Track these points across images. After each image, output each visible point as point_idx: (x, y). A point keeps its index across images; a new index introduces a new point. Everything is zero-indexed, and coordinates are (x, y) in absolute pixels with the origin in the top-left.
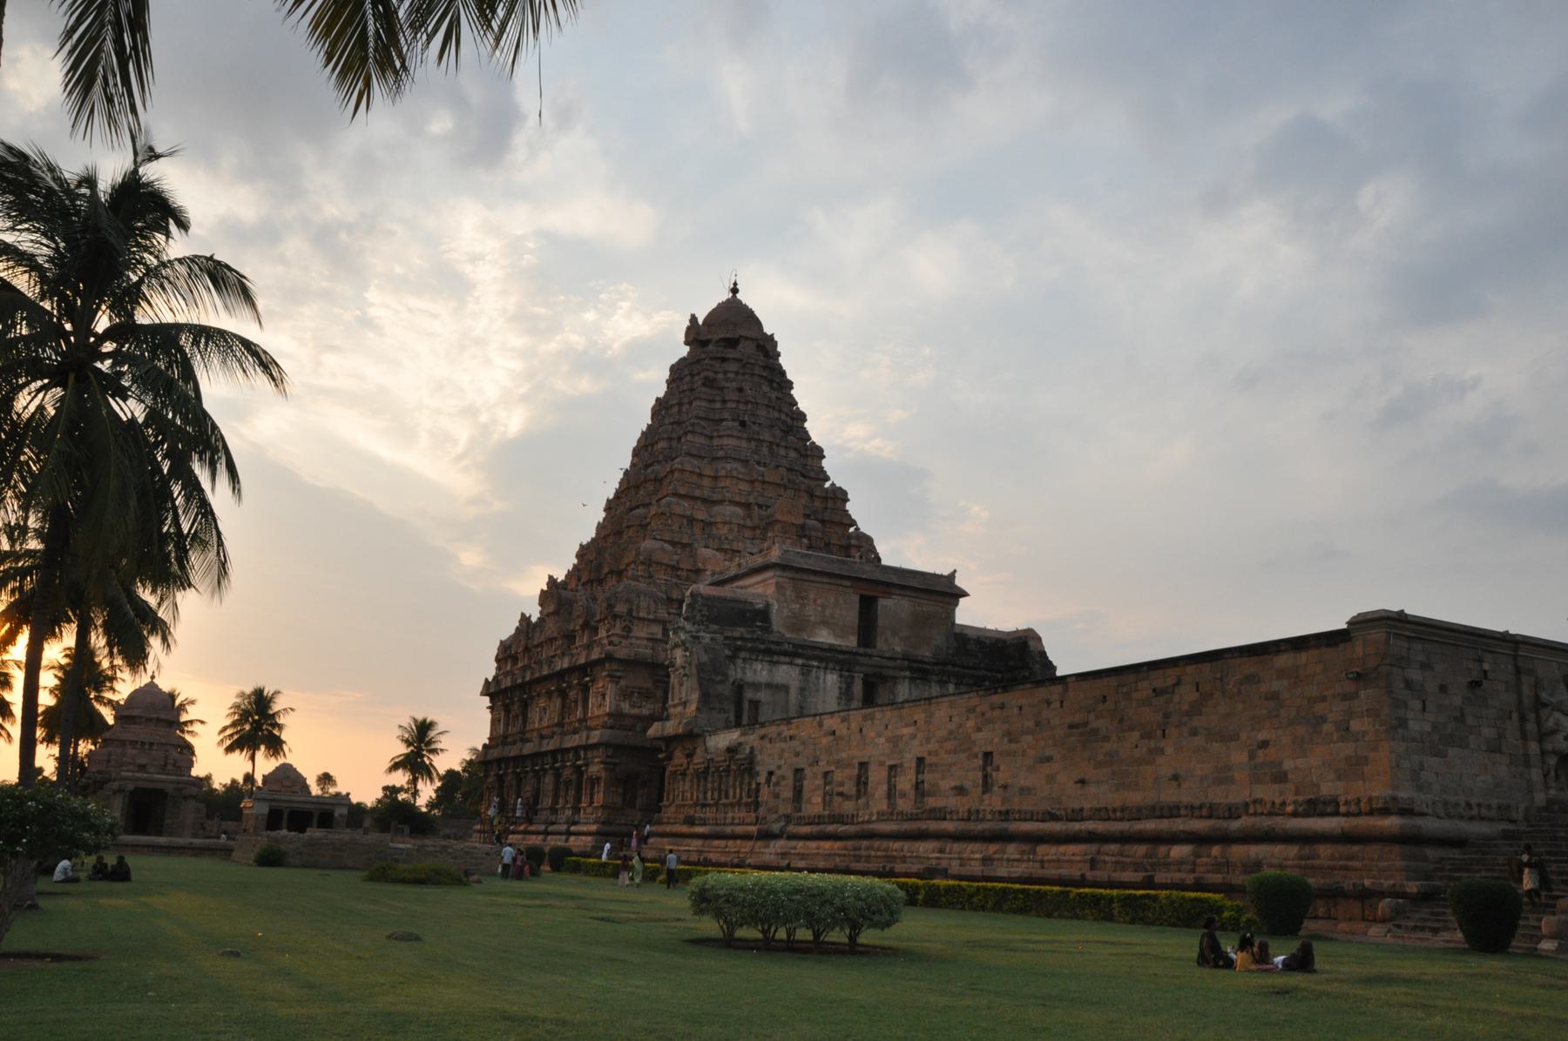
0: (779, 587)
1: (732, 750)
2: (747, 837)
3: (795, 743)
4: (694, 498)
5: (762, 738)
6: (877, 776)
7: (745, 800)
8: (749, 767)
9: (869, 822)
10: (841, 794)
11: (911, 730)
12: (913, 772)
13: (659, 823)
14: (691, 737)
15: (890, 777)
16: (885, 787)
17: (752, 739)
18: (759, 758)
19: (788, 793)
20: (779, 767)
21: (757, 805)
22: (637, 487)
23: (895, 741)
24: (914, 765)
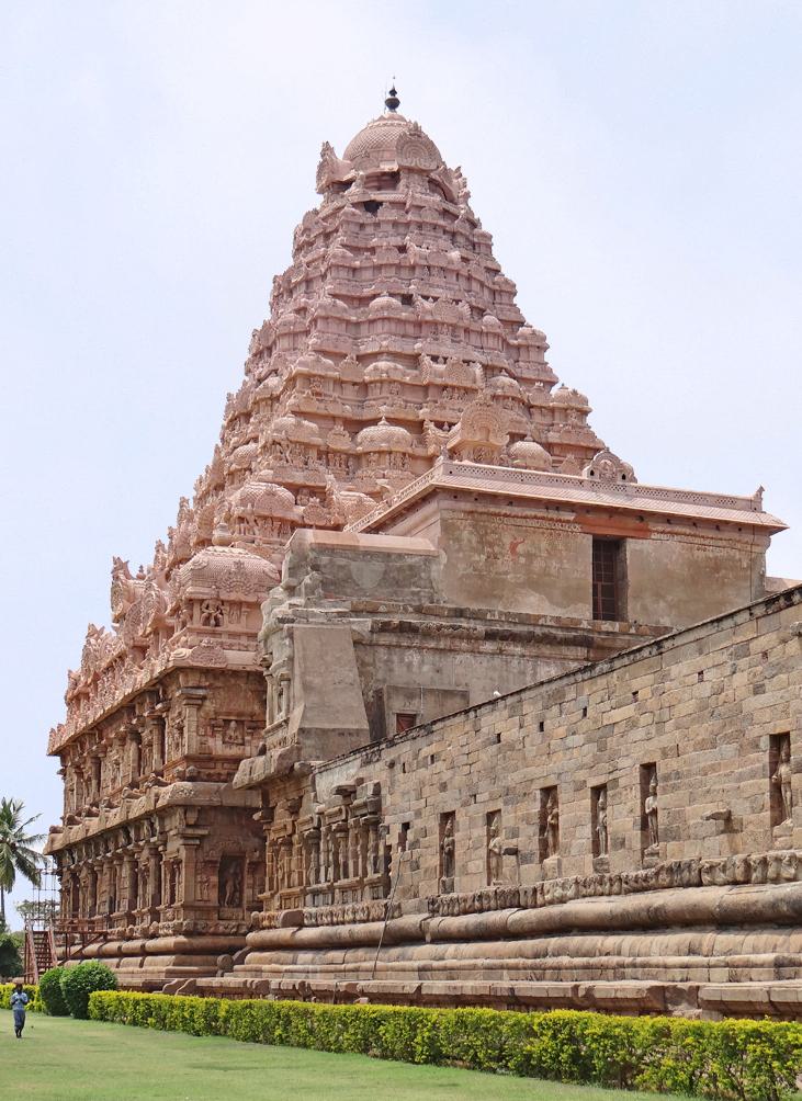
0: (447, 528)
1: (346, 793)
2: (369, 943)
3: (440, 766)
4: (334, 418)
5: (392, 765)
6: (573, 810)
7: (372, 876)
8: (374, 825)
9: (562, 900)
10: (514, 852)
11: (629, 711)
12: (636, 792)
13: (256, 926)
14: (291, 778)
15: (595, 810)
16: (587, 831)
17: (377, 772)
18: (387, 801)
19: (433, 860)
20: (418, 814)
21: (387, 884)
22: (248, 415)
23: (601, 737)
24: (636, 776)
